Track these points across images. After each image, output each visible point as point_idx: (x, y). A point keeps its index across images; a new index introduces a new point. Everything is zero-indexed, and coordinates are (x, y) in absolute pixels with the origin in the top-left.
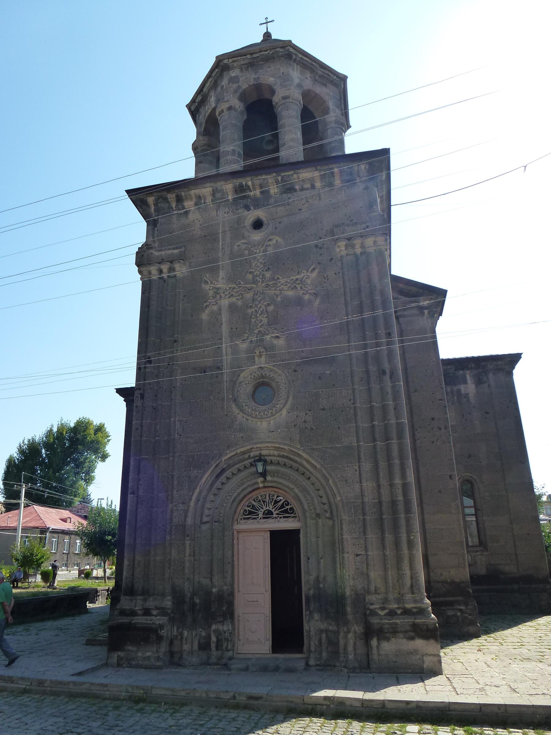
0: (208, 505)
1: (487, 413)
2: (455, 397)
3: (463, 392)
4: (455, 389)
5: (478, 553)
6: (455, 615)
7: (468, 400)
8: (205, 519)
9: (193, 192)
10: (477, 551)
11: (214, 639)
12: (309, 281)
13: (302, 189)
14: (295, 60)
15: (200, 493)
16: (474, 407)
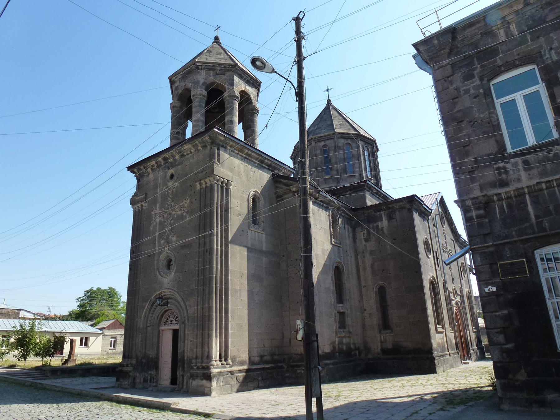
0: (149, 319)
1: (394, 240)
4: (375, 225)
6: (301, 372)
7: (383, 232)
8: (148, 325)
9: (149, 164)
11: (149, 378)
12: (186, 206)
13: (188, 154)
14: (201, 69)
15: (145, 313)
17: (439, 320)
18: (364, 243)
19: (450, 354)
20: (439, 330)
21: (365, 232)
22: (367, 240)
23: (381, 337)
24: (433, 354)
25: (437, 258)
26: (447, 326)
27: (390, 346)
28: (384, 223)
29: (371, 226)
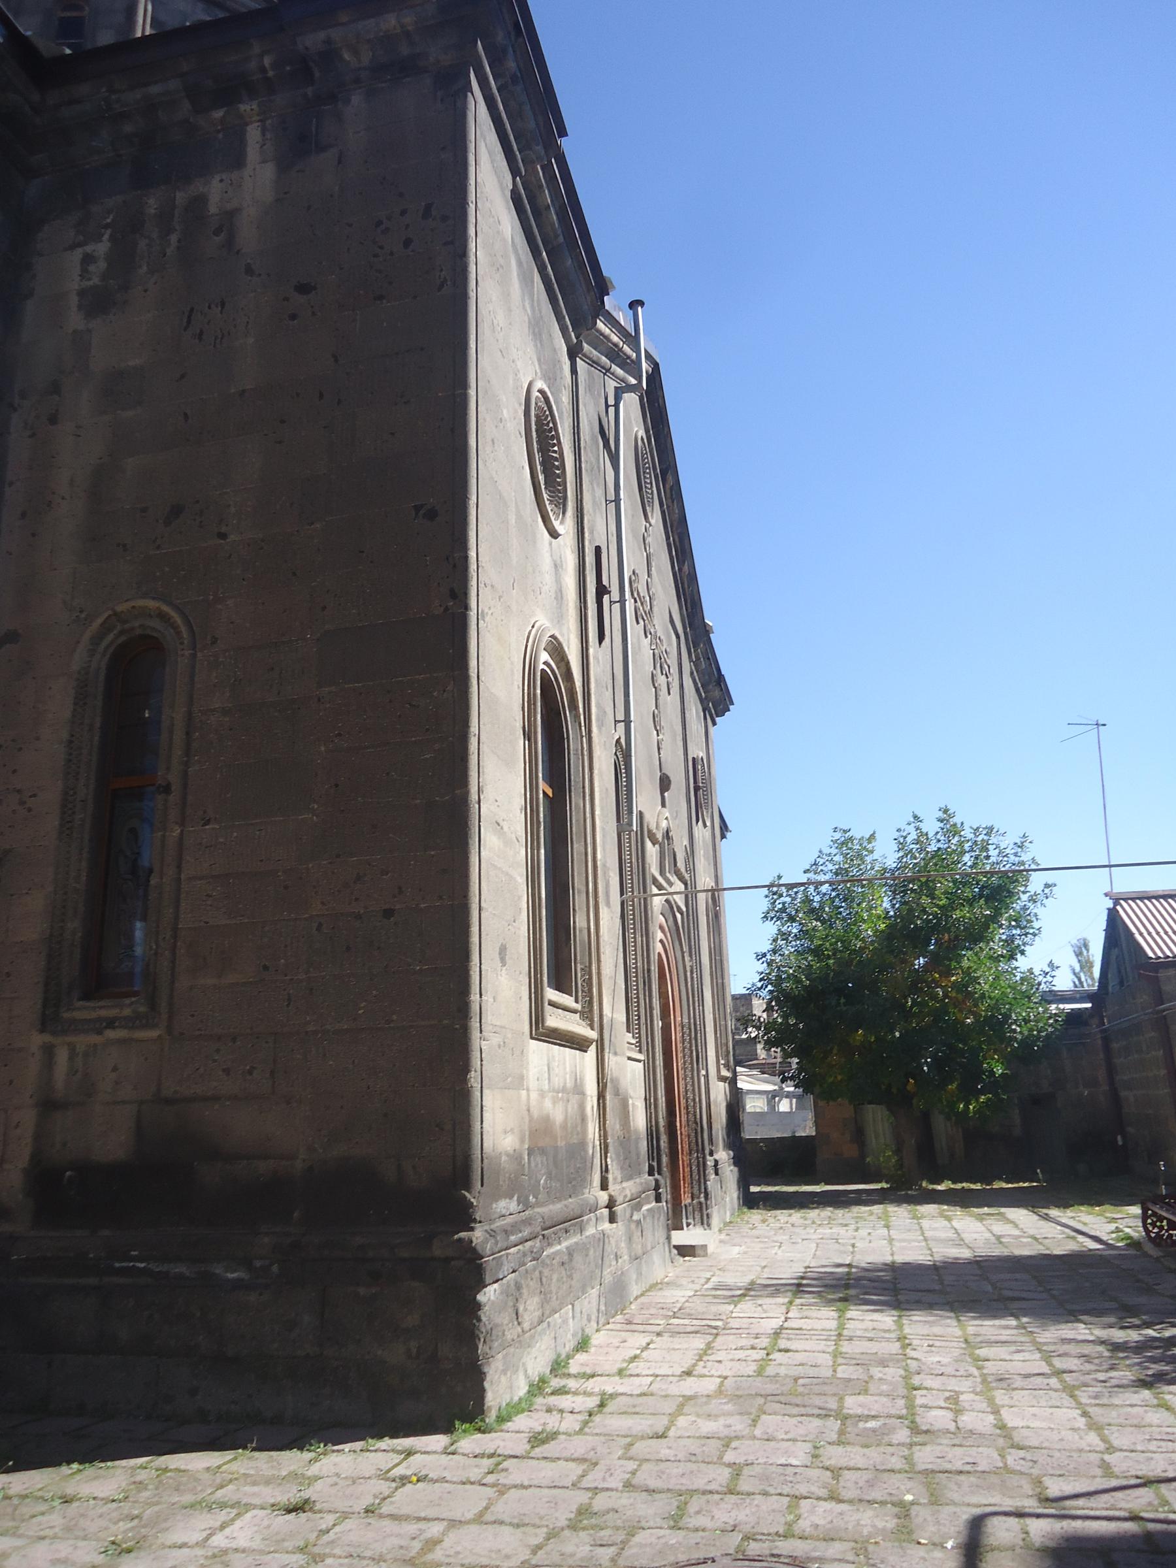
2: (174, 238)
3: (213, 209)
4: (181, 197)
5: (111, 1034)
10: (111, 1023)
16: (249, 270)
17: (559, 958)
18: (75, 320)
19: (611, 1205)
20: (553, 1020)
21: (101, 248)
22: (98, 302)
23: (49, 1051)
24: (465, 1218)
25: (601, 591)
26: (613, 1009)
27: (108, 1138)
28: (250, 186)
29: (152, 205)
